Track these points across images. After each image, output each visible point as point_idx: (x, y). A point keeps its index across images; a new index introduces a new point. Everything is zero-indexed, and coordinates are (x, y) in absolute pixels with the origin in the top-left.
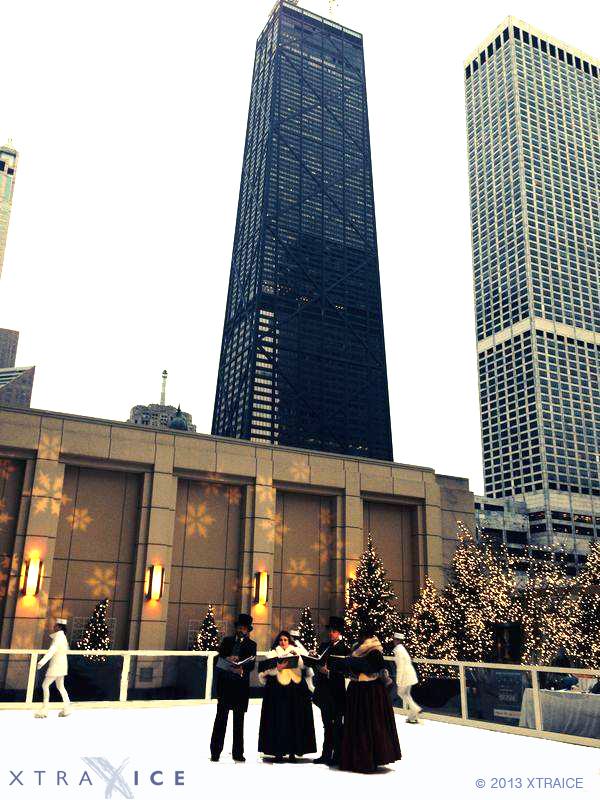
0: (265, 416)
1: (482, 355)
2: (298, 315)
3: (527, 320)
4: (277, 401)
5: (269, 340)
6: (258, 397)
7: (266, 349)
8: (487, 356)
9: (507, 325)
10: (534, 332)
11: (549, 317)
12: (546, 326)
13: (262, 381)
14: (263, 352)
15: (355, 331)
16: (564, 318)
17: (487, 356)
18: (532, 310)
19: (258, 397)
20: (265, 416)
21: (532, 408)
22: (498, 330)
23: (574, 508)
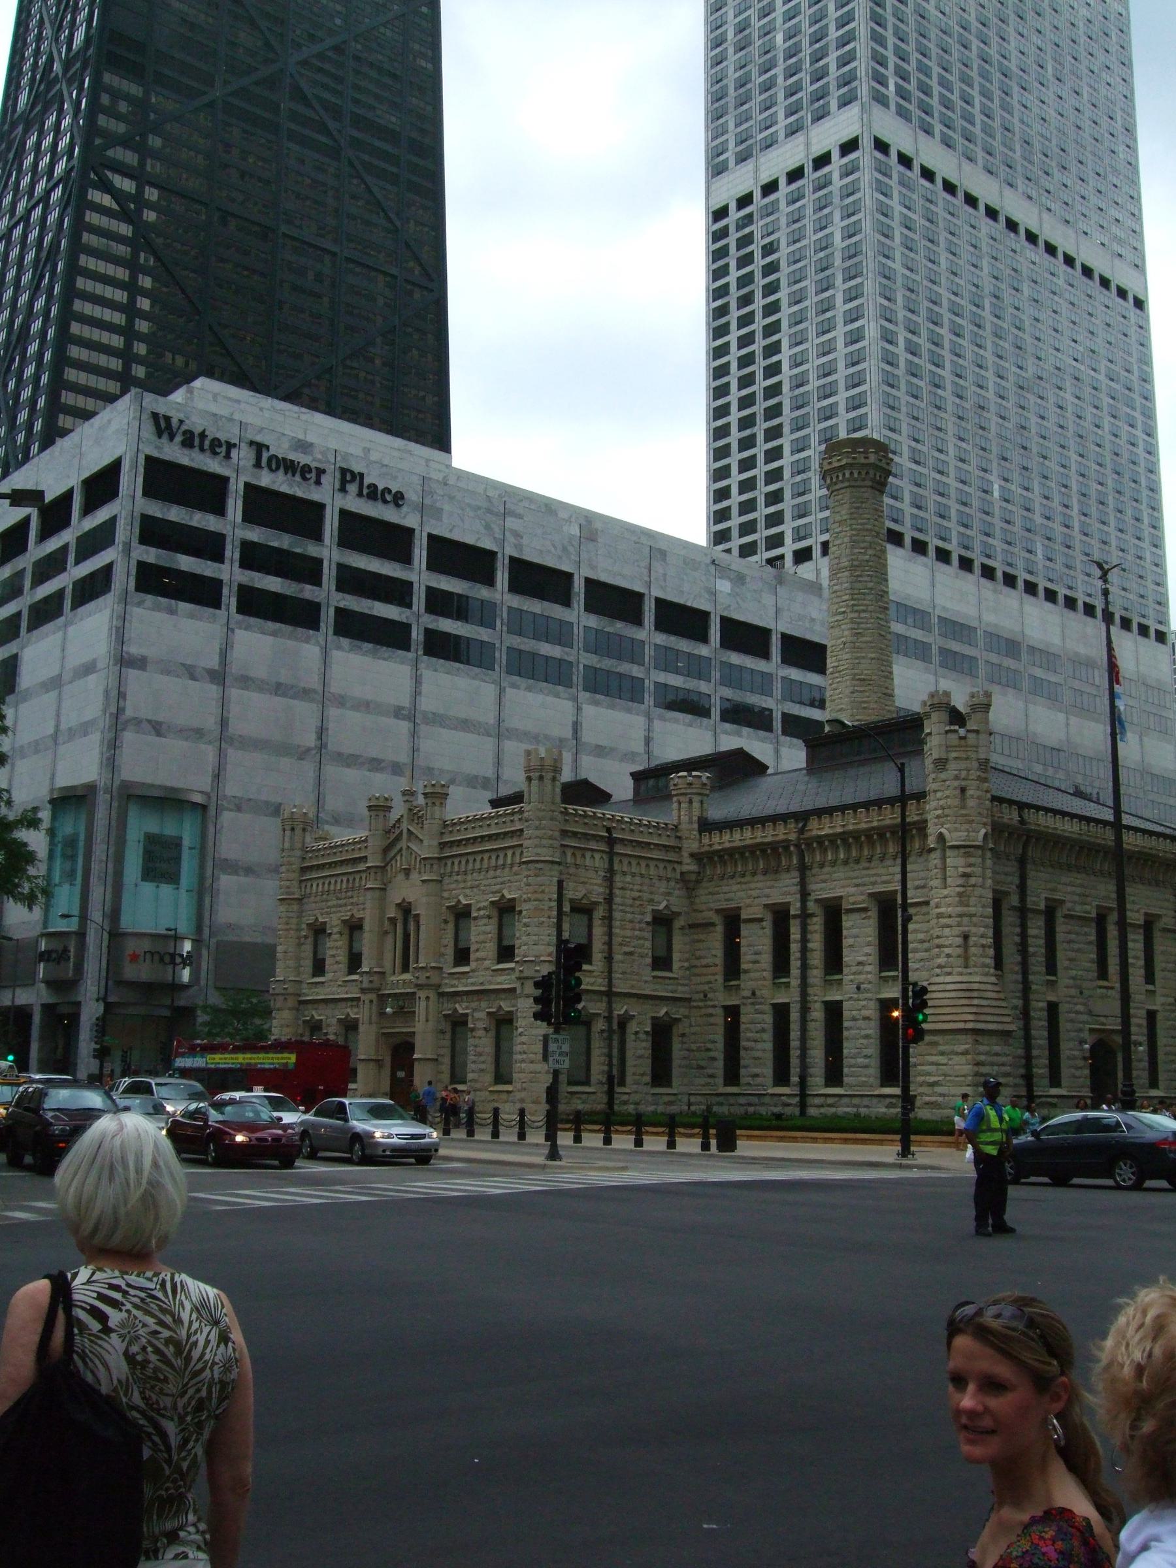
0: (103, 360)
1: (719, 214)
2: (211, 105)
3: (854, 110)
4: (143, 326)
5: (130, 158)
6: (88, 309)
7: (119, 182)
8: (734, 215)
9: (792, 131)
10: (866, 143)
11: (903, 113)
12: (901, 137)
13: (102, 267)
14: (107, 188)
15: (369, 179)
16: (938, 128)
17: (734, 215)
18: (864, 88)
19: (88, 309)
20: (103, 360)
21: (855, 337)
22: (769, 144)
23: (939, 601)
